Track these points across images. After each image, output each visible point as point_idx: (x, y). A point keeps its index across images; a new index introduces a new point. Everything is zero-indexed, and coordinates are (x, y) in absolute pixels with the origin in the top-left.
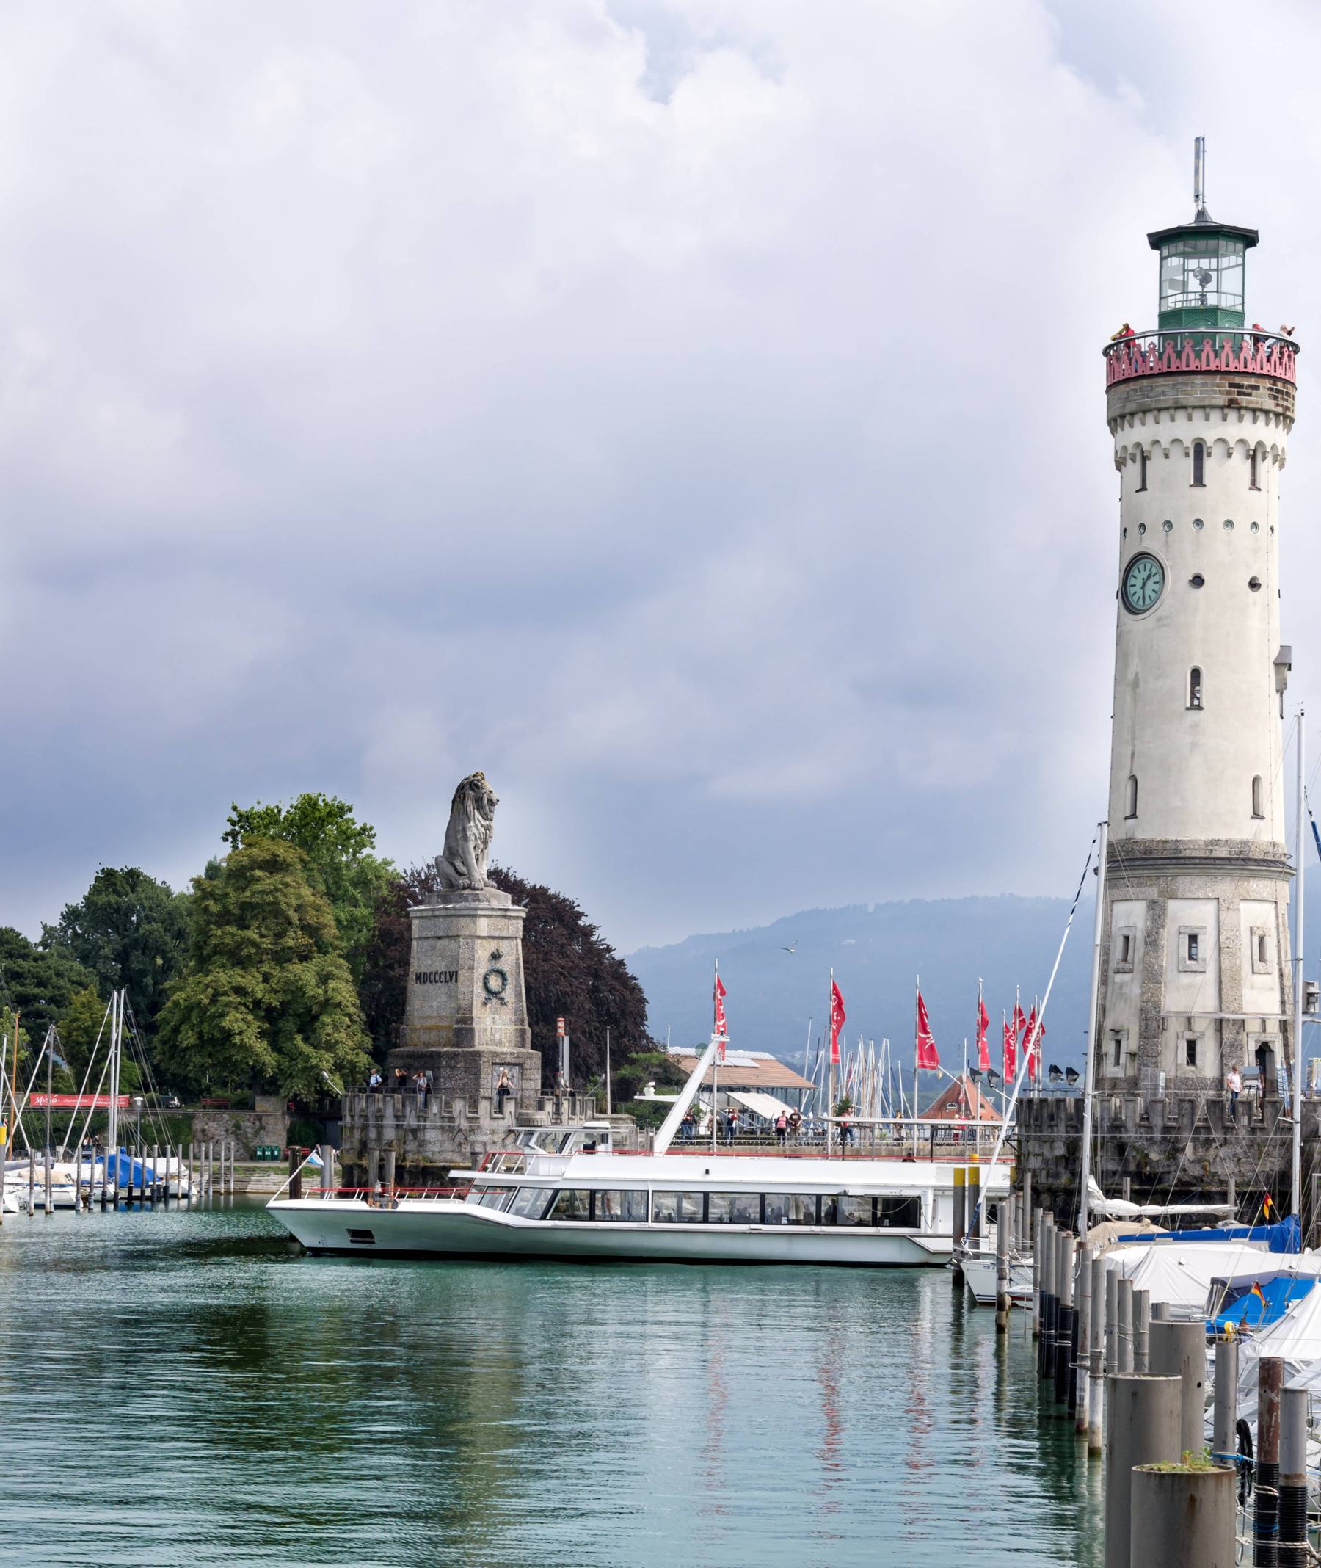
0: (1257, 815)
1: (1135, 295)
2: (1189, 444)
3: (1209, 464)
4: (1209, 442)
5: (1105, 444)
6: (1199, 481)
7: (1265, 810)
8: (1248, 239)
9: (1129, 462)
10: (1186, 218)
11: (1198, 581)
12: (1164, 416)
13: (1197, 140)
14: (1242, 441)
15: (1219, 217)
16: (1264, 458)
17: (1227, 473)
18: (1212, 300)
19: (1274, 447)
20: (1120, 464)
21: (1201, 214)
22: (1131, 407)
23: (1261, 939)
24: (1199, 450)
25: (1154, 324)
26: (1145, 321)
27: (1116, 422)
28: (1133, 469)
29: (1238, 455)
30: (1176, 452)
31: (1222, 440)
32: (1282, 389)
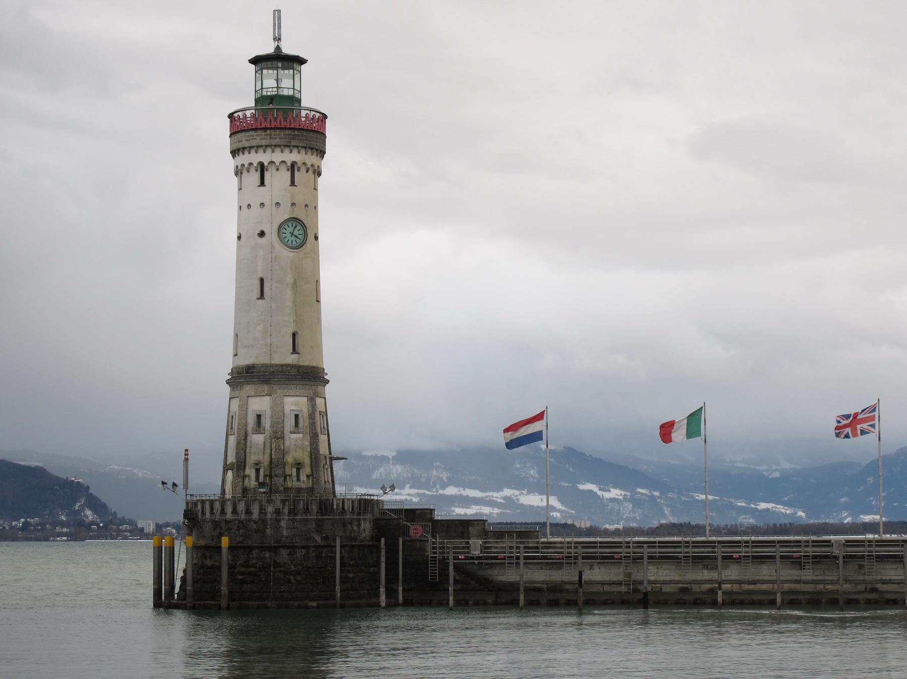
0: (295, 351)
2: (255, 165)
3: (267, 175)
4: (266, 164)
6: (262, 183)
7: (299, 348)
11: (262, 234)
13: (274, 11)
14: (283, 162)
16: (298, 170)
17: (278, 179)
19: (304, 164)
21: (278, 48)
22: (240, 145)
23: (297, 416)
25: (252, 104)
29: (283, 169)
30: (252, 170)
31: (272, 162)
32: (321, 135)
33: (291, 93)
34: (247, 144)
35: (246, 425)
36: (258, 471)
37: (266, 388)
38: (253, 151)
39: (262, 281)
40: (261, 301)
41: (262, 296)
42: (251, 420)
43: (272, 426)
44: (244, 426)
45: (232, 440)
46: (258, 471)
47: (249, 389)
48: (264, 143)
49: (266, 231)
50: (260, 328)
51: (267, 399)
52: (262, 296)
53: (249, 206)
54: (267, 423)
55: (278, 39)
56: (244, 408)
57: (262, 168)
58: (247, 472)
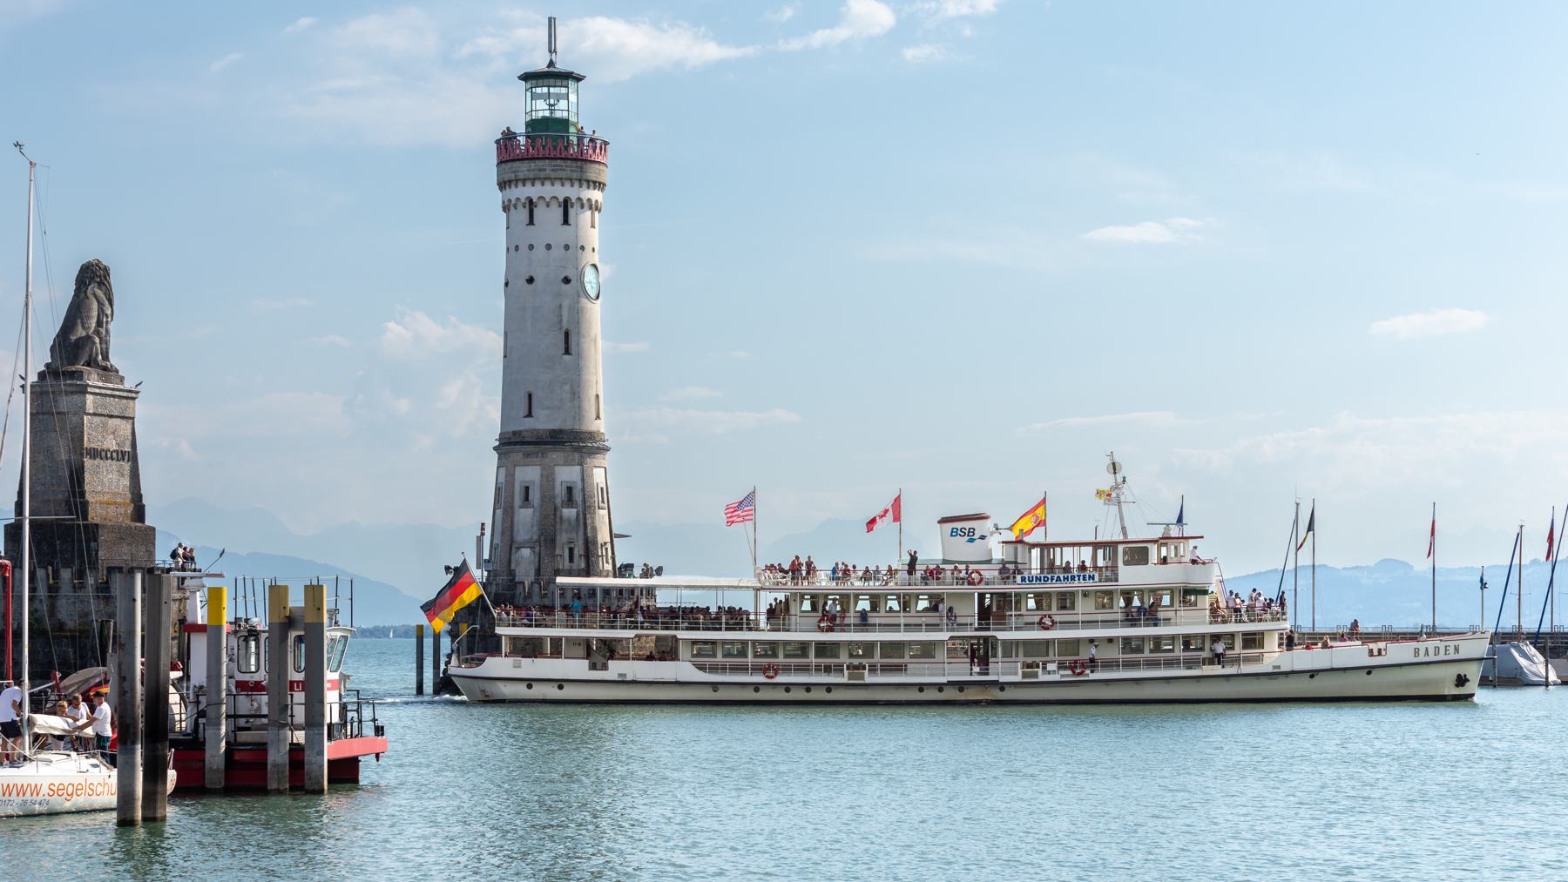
1: (516, 110)
3: (572, 212)
5: (498, 197)
6: (566, 222)
8: (578, 79)
9: (520, 206)
10: (541, 65)
11: (567, 280)
12: (548, 183)
15: (561, 66)
18: (558, 115)
20: (506, 208)
21: (551, 64)
24: (566, 204)
26: (520, 128)
27: (503, 185)
28: (524, 213)
31: (579, 199)
33: (565, 114)
34: (553, 175)
35: (554, 497)
36: (571, 550)
37: (576, 455)
38: (528, 184)
39: (567, 334)
40: (567, 357)
41: (567, 352)
42: (560, 492)
43: (584, 501)
44: (548, 497)
45: (525, 517)
46: (571, 550)
47: (555, 456)
48: (575, 175)
49: (571, 276)
50: (567, 387)
51: (578, 468)
52: (567, 352)
53: (549, 247)
54: (578, 496)
55: (552, 51)
56: (548, 478)
57: (566, 204)
58: (558, 552)
